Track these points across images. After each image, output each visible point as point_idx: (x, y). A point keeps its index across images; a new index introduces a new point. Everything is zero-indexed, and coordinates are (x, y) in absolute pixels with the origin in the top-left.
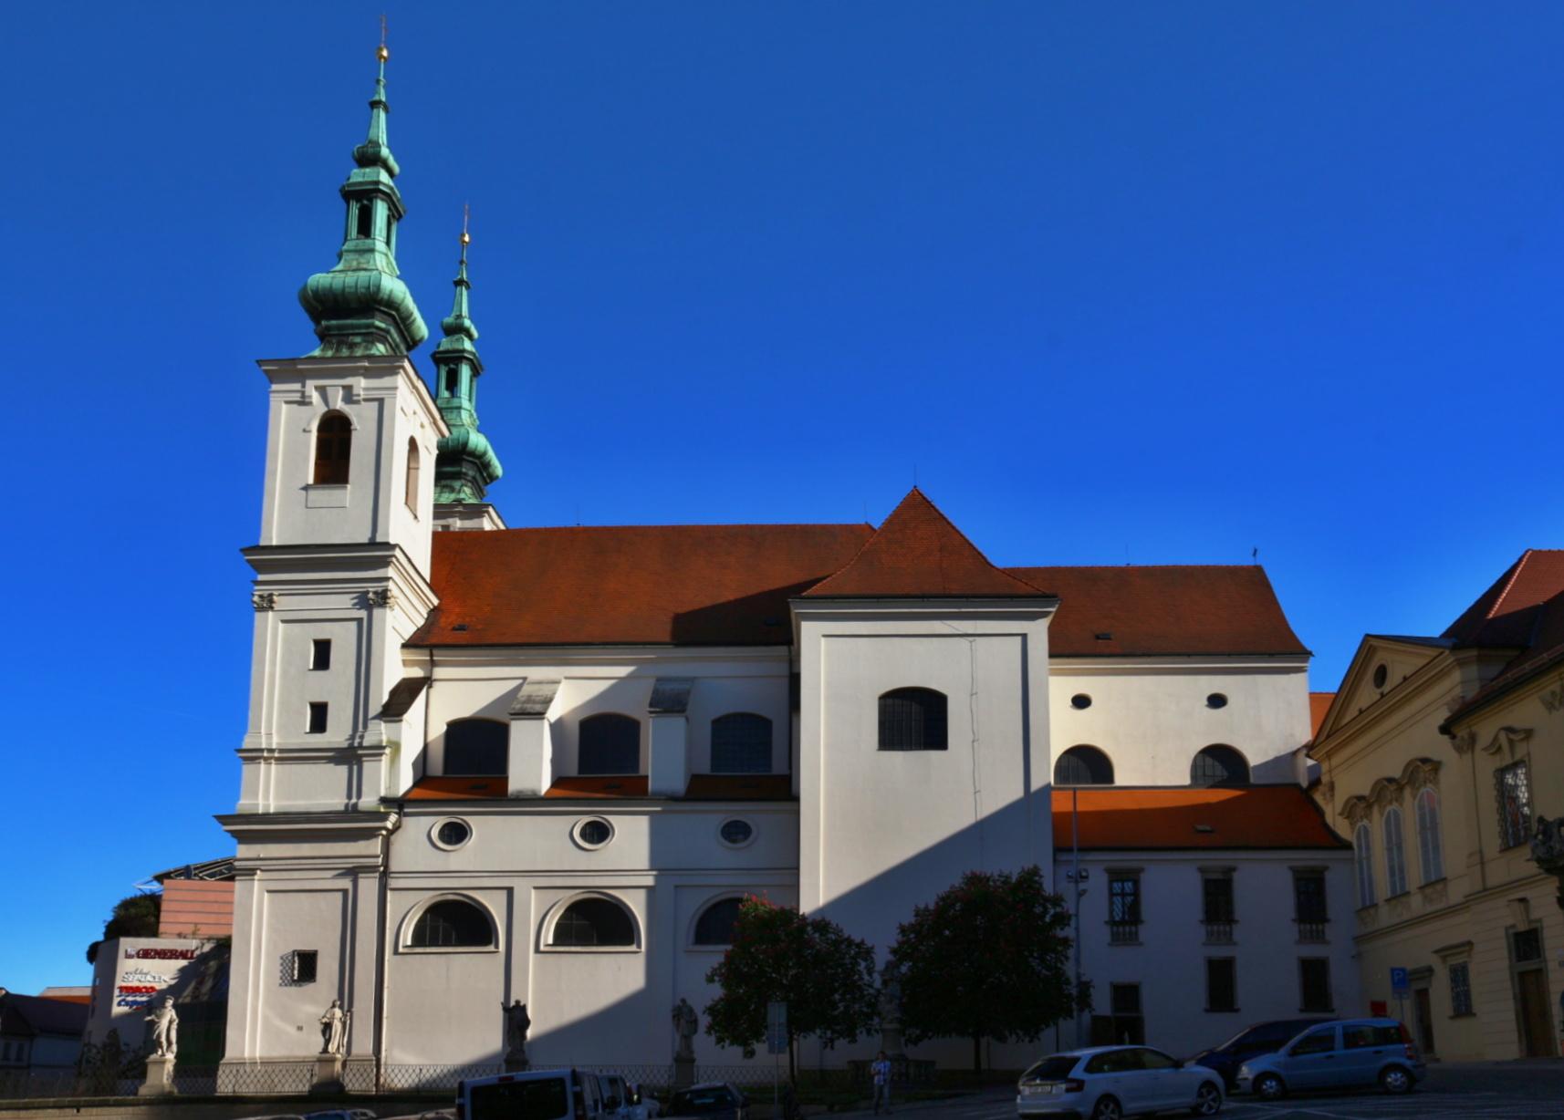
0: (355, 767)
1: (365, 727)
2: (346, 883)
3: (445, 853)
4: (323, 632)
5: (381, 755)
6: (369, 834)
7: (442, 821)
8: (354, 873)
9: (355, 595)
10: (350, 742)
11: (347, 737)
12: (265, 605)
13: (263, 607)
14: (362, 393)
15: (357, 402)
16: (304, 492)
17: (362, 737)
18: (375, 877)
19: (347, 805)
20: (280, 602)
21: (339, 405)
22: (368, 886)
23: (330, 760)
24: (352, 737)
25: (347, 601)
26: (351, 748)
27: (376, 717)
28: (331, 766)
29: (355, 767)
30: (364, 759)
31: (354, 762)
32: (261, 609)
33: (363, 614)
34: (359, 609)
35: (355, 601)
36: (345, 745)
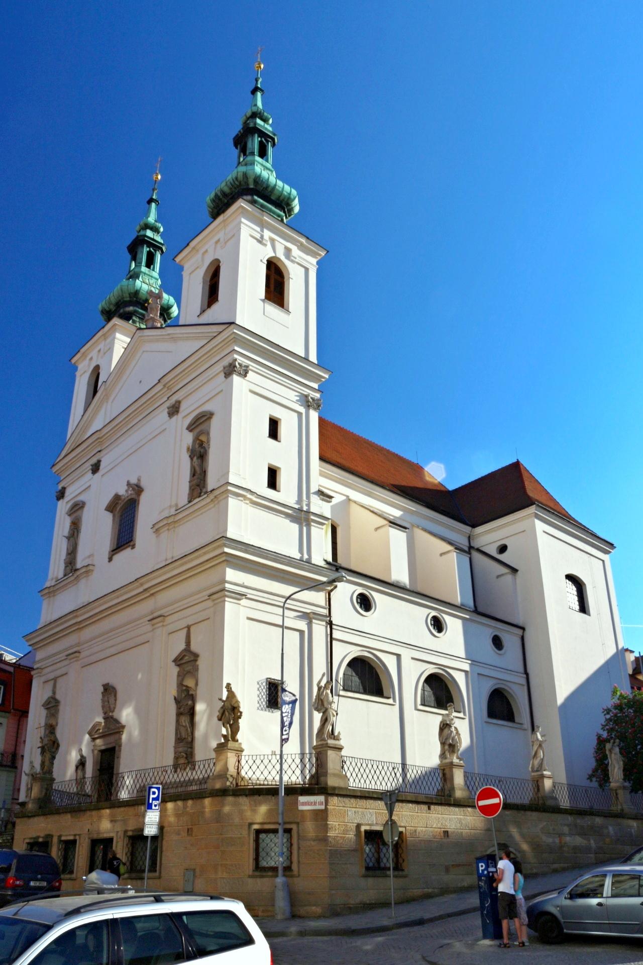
0: (305, 529)
1: (308, 497)
2: (302, 625)
3: (362, 617)
4: (278, 413)
5: (323, 524)
6: (315, 586)
7: (360, 590)
8: (308, 617)
9: (297, 394)
10: (299, 506)
11: (295, 502)
12: (242, 372)
13: (240, 373)
14: (297, 258)
15: (293, 261)
16: (262, 303)
17: (308, 505)
18: (324, 625)
19: (302, 557)
20: (250, 374)
21: (281, 255)
22: (319, 629)
23: (287, 515)
24: (299, 501)
25: (293, 396)
26: (300, 510)
27: (314, 493)
28: (287, 522)
29: (305, 529)
30: (312, 524)
31: (304, 524)
32: (240, 374)
33: (302, 410)
34: (300, 405)
35: (298, 398)
36: (297, 506)
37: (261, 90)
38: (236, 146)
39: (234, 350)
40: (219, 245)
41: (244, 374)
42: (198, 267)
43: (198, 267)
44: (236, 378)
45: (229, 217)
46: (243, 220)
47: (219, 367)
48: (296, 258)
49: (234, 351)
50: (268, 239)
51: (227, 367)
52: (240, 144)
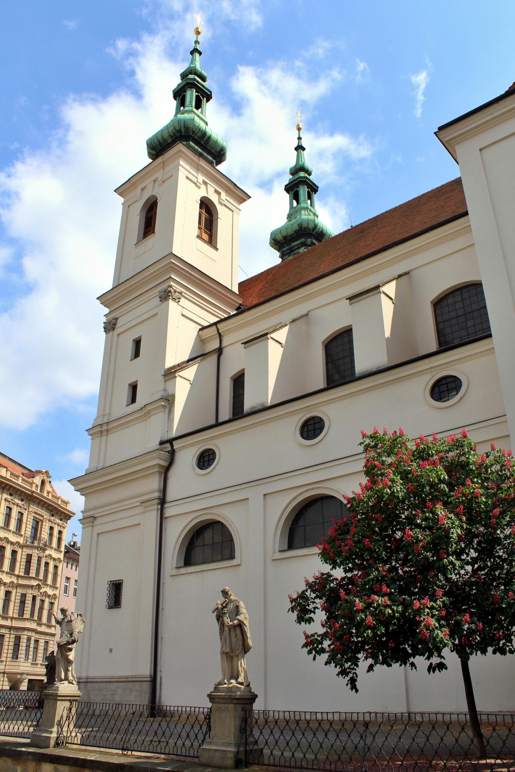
32: (174, 299)
37: (200, 53)
38: (175, 98)
39: (171, 277)
40: (157, 183)
41: (177, 300)
42: (136, 201)
43: (136, 201)
44: (172, 304)
45: (167, 159)
46: (182, 163)
47: (156, 291)
48: (224, 201)
49: (170, 278)
50: (201, 182)
51: (162, 292)
52: (179, 96)
